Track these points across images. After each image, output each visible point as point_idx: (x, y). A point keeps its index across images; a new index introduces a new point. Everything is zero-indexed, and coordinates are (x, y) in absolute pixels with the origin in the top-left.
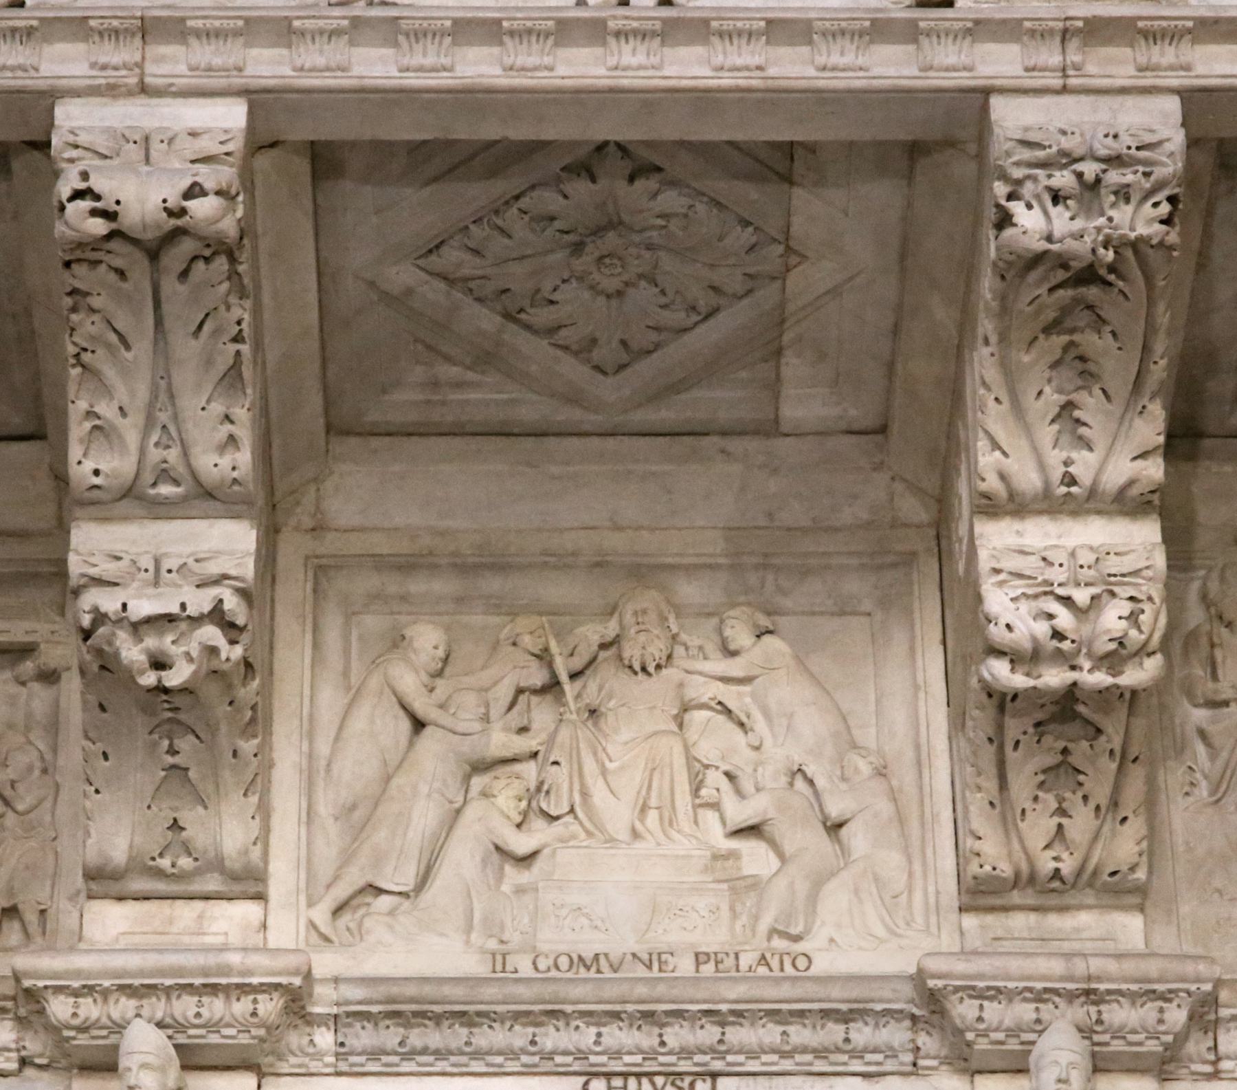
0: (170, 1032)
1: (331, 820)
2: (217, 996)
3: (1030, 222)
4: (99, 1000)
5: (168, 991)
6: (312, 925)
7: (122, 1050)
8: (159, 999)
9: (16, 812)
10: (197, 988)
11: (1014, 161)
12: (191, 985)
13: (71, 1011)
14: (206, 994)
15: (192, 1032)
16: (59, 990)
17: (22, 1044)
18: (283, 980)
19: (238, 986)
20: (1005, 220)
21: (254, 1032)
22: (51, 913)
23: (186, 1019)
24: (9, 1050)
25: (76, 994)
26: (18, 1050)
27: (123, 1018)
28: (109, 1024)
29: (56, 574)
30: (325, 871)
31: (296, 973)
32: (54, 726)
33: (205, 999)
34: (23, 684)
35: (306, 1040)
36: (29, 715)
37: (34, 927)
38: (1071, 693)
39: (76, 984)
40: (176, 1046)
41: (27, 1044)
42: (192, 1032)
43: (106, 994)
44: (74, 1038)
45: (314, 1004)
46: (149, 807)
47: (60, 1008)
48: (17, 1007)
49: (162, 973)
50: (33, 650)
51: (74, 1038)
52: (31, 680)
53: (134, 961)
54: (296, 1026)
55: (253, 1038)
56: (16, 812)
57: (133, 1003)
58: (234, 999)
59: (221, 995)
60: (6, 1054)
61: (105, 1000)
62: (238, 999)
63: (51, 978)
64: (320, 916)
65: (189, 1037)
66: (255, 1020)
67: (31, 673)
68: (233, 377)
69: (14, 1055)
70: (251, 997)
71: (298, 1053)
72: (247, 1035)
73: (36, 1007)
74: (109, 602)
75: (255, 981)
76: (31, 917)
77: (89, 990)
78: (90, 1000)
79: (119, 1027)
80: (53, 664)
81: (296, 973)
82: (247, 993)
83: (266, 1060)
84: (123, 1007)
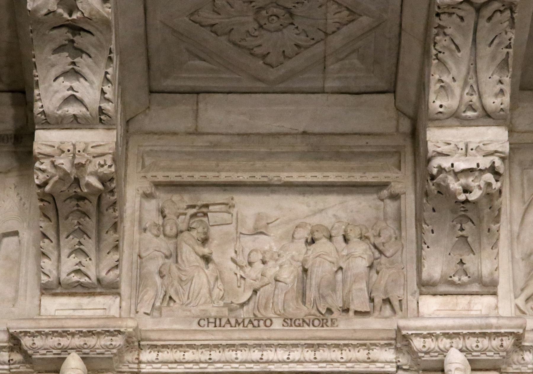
0: (465, 353)
1: (521, 260)
2: (485, 338)
4: (434, 340)
5: (464, 335)
6: (517, 307)
7: (445, 362)
8: (460, 339)
9: (386, 256)
10: (477, 334)
12: (475, 333)
13: (422, 344)
14: (482, 337)
15: (474, 354)
16: (417, 335)
17: (398, 359)
18: (515, 331)
19: (495, 333)
21: (501, 354)
22: (404, 302)
23: (472, 347)
24: (391, 362)
25: (425, 337)
26: (396, 362)
27: (445, 347)
28: (438, 350)
29: (396, 152)
30: (520, 284)
31: (520, 327)
32: (399, 219)
33: (480, 339)
34: (382, 200)
35: (520, 357)
36: (385, 214)
37: (397, 308)
39: (425, 333)
40: (469, 360)
41: (400, 360)
42: (474, 354)
43: (437, 337)
44: (423, 357)
45: (525, 341)
46: (450, 254)
47: (417, 343)
48: (397, 343)
49: (462, 327)
50: (387, 185)
51: (423, 357)
52: (386, 198)
53: (450, 322)
54: (516, 352)
55: (501, 356)
56: (386, 256)
57: (448, 341)
58: (492, 339)
59: (487, 338)
60: (391, 364)
61: (437, 339)
62: (494, 339)
63: (414, 330)
64: (520, 301)
65: (473, 356)
66: (502, 349)
67: (386, 196)
69: (394, 365)
70: (500, 338)
71: (517, 363)
72: (498, 355)
73: (405, 343)
75: (503, 331)
76: (396, 303)
77: (431, 335)
78: (430, 340)
79: (444, 352)
80: (397, 192)
81: (520, 327)
82: (498, 337)
83: (503, 366)
84: (445, 343)
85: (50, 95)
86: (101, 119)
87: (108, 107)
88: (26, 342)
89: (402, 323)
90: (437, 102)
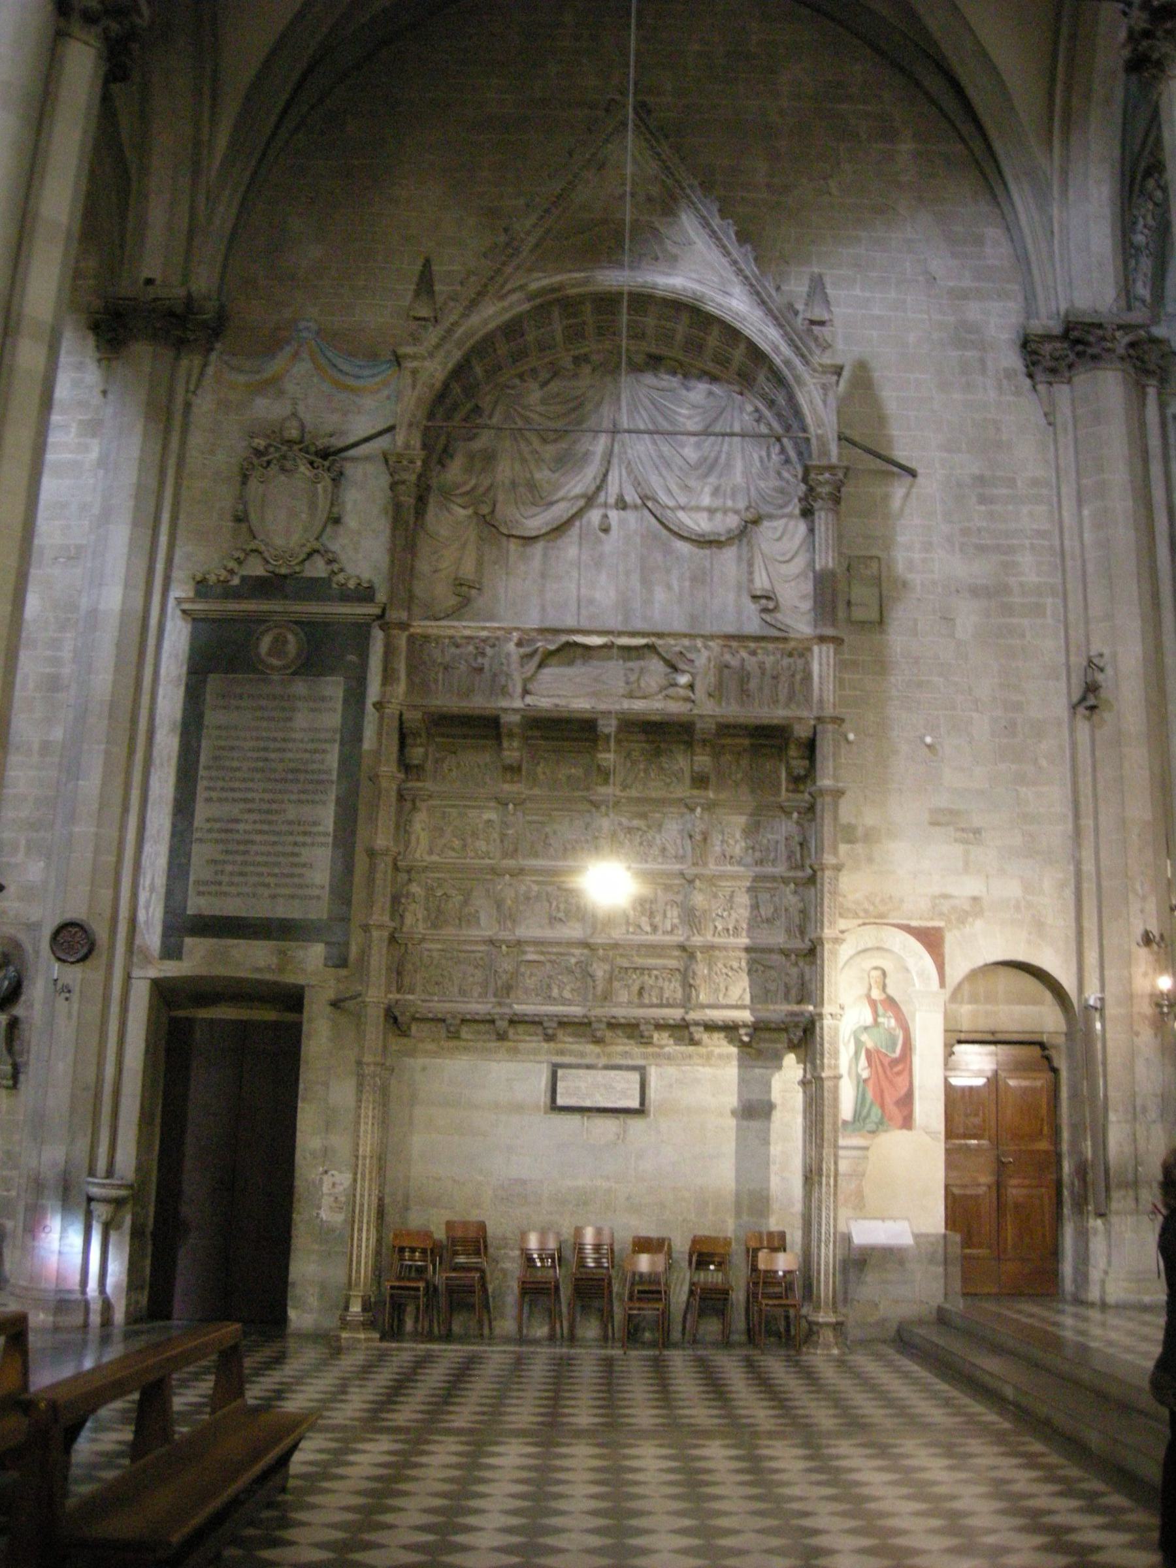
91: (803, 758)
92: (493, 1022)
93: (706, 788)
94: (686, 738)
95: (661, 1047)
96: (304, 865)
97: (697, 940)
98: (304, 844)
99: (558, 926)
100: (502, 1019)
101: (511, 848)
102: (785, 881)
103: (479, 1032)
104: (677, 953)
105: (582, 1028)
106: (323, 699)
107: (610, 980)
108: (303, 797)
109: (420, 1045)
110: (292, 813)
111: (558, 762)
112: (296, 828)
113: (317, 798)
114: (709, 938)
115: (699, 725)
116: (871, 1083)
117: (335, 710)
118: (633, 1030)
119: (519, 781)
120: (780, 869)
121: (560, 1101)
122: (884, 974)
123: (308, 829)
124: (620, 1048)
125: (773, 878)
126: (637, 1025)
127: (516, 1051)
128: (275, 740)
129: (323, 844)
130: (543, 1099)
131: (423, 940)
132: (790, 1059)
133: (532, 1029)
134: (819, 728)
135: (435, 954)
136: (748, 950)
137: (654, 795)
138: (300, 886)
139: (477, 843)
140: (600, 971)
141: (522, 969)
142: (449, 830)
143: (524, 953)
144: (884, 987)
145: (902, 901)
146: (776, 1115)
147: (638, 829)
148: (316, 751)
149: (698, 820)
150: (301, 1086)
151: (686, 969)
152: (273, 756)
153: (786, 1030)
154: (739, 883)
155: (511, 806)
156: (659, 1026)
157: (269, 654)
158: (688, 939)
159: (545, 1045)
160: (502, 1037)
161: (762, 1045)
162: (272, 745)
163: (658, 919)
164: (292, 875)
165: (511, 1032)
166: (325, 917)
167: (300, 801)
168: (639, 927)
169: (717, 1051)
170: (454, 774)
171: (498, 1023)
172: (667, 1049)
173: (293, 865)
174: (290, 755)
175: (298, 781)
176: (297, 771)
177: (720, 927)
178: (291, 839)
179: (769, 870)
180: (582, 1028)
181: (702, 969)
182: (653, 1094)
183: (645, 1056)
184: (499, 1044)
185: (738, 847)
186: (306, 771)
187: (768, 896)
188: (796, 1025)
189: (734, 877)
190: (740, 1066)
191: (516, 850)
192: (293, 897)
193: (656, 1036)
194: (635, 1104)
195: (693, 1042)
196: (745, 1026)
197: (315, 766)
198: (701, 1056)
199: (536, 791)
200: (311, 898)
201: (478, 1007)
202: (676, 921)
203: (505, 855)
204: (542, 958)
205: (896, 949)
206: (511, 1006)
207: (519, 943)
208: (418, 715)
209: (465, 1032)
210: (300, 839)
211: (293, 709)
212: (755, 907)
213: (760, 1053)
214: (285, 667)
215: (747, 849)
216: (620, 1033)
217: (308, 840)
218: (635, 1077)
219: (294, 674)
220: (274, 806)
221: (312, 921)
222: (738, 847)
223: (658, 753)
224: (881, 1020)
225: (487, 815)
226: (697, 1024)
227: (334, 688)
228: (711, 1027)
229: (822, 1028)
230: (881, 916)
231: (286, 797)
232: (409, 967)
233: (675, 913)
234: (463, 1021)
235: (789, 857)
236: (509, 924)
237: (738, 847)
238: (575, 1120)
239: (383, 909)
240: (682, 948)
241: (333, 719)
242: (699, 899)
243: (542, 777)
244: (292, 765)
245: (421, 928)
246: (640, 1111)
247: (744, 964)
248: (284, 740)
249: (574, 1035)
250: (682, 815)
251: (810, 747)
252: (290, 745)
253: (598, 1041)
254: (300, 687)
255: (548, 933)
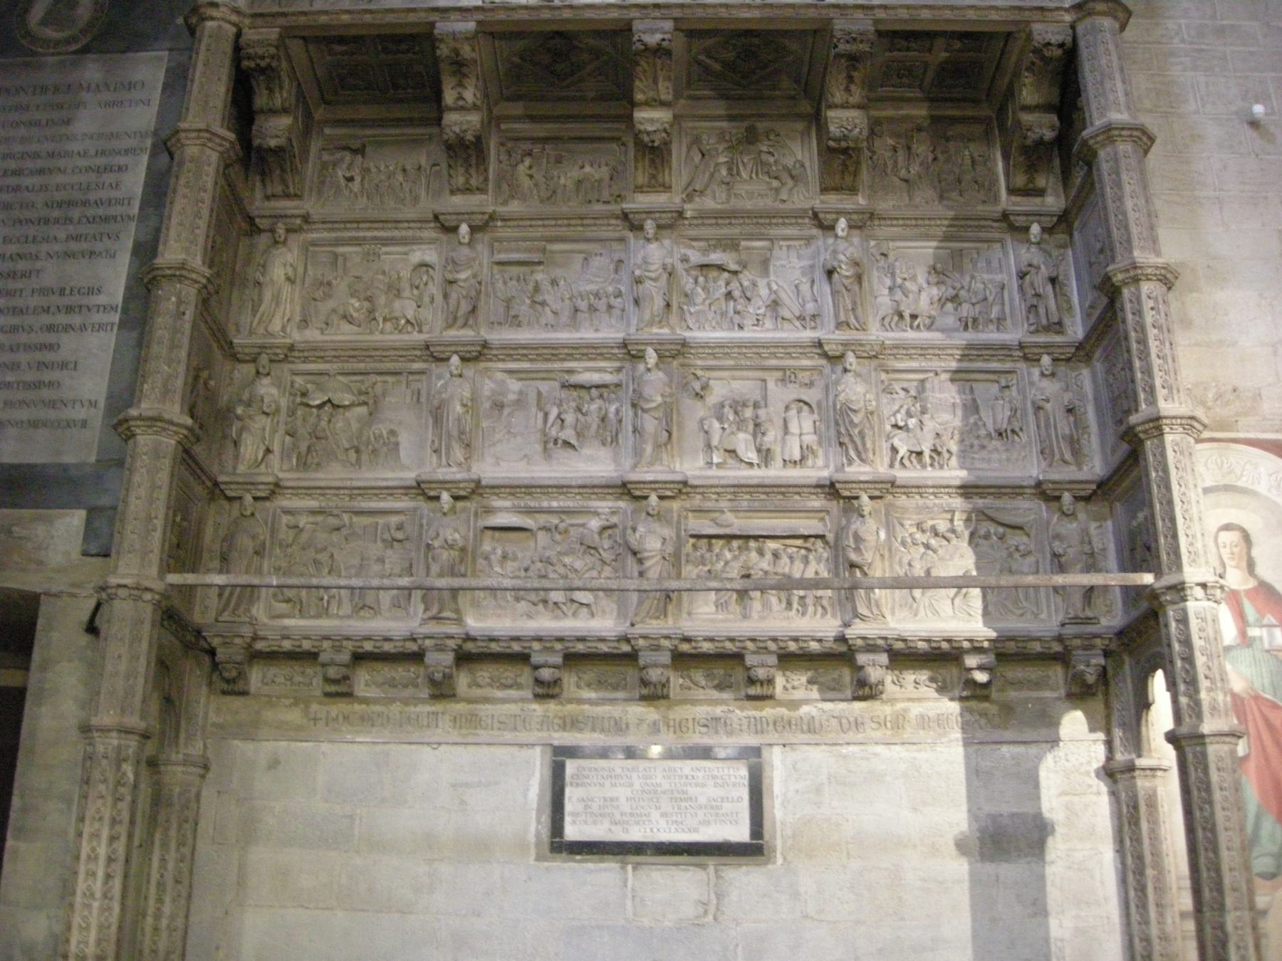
3: (842, 47)
11: (838, 34)
20: (836, 46)
38: (848, 148)
68: (669, 79)
74: (642, 128)
85: (449, 97)
86: (475, 107)
87: (478, 103)
88: (441, 217)
89: (624, 206)
90: (639, 97)
91: (1046, 108)
92: (417, 657)
93: (853, 190)
94: (806, 107)
95: (794, 705)
96: (64, 365)
97: (858, 471)
98: (68, 328)
99: (562, 453)
100: (440, 648)
101: (465, 307)
102: (1028, 354)
103: (392, 684)
104: (817, 503)
105: (614, 663)
106: (131, 86)
107: (675, 560)
108: (74, 246)
109: (269, 714)
110: (51, 274)
111: (559, 161)
112: (56, 300)
113: (99, 246)
114: (880, 467)
115: (839, 25)
116: (1252, 765)
117: (147, 103)
118: (727, 665)
119: (481, 190)
120: (1012, 336)
121: (572, 832)
122: (1247, 538)
123: (75, 300)
124: (701, 711)
125: (1003, 350)
126: (738, 657)
127: (473, 721)
128: (36, 155)
129: (102, 327)
130: (534, 826)
131: (277, 488)
132: (1074, 722)
133: (508, 672)
134: (1080, 29)
135: (303, 521)
136: (967, 490)
137: (748, 205)
138: (52, 404)
139: (397, 304)
140: (652, 539)
141: (487, 547)
142: (341, 287)
143: (489, 511)
144: (1251, 566)
145: (1258, 396)
146: (1056, 847)
147: (721, 268)
148: (108, 169)
149: (845, 246)
150: (16, 802)
151: (840, 532)
152: (28, 181)
153: (1063, 658)
154: (936, 364)
155: (464, 229)
156: (791, 658)
157: (44, 23)
158: (840, 468)
159: (537, 708)
160: (442, 690)
161: (1013, 694)
162: (29, 164)
163: (772, 436)
164: (37, 385)
165: (462, 681)
166: (93, 459)
167: (69, 255)
168: (732, 452)
169: (916, 710)
170: (356, 186)
171: (431, 658)
172: (805, 709)
173: (42, 365)
174: (60, 179)
175: (69, 220)
176: (71, 203)
177: (903, 451)
178: (46, 319)
179: (992, 336)
180: (614, 663)
181: (871, 530)
182: (778, 811)
183: (758, 727)
184: (438, 707)
185: (924, 298)
186: (85, 203)
187: (995, 388)
188: (1088, 642)
189: (924, 350)
190: (967, 743)
191: (474, 310)
192: (34, 424)
193: (780, 681)
194: (741, 833)
195: (865, 691)
196: (978, 650)
197: (103, 194)
198: (881, 724)
199: (515, 207)
200: (69, 424)
201: (391, 625)
202: (810, 439)
203: (452, 322)
204: (527, 522)
205: (1262, 488)
206: (459, 621)
207: (478, 488)
208: (273, 34)
209: (363, 681)
210: (62, 319)
211: (79, 105)
212: (972, 408)
213: (1008, 710)
214: (68, 42)
215: (942, 302)
216: (699, 676)
217: (76, 320)
218: (741, 772)
219: (85, 50)
220: (21, 265)
221: (65, 468)
222: (924, 298)
223: (751, 137)
224: (1253, 632)
225: (417, 256)
226: (871, 648)
227: (149, 69)
228: (904, 656)
229: (1184, 620)
230: (1223, 425)
231: (45, 247)
232: (244, 542)
233: (808, 426)
234: (360, 658)
235: (1033, 308)
236: (458, 453)
237: (925, 297)
238: (605, 872)
239: (166, 392)
240: (831, 489)
241: (142, 117)
242: (855, 390)
243: (526, 183)
244: (60, 196)
245: (277, 469)
246: (752, 850)
247: (959, 524)
248: (51, 155)
249: (600, 684)
250: (809, 240)
251: (1065, 72)
252: (62, 163)
253: (654, 694)
254: (92, 71)
255: (544, 472)
